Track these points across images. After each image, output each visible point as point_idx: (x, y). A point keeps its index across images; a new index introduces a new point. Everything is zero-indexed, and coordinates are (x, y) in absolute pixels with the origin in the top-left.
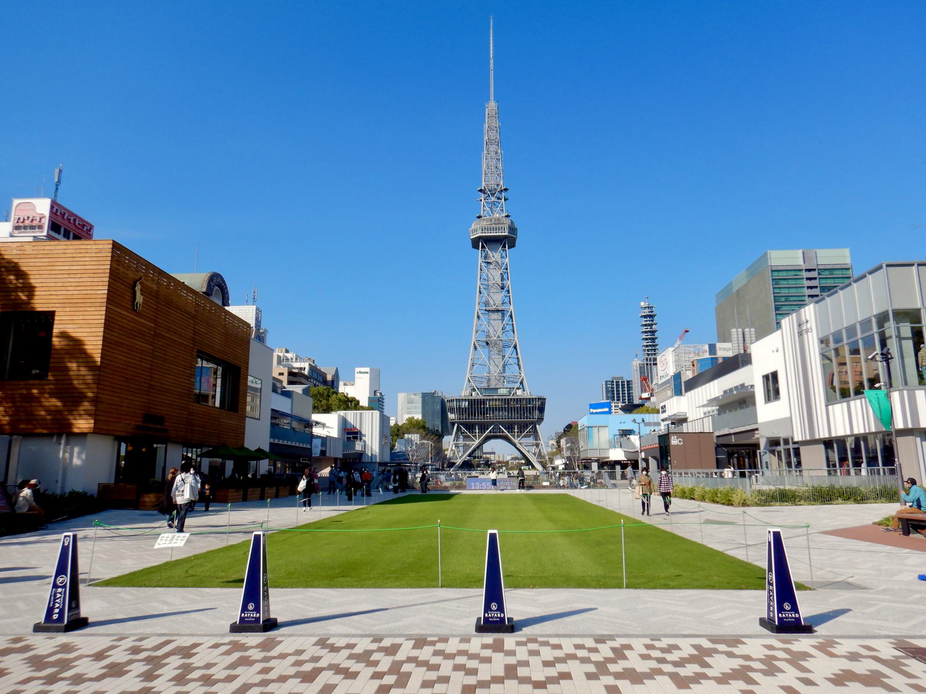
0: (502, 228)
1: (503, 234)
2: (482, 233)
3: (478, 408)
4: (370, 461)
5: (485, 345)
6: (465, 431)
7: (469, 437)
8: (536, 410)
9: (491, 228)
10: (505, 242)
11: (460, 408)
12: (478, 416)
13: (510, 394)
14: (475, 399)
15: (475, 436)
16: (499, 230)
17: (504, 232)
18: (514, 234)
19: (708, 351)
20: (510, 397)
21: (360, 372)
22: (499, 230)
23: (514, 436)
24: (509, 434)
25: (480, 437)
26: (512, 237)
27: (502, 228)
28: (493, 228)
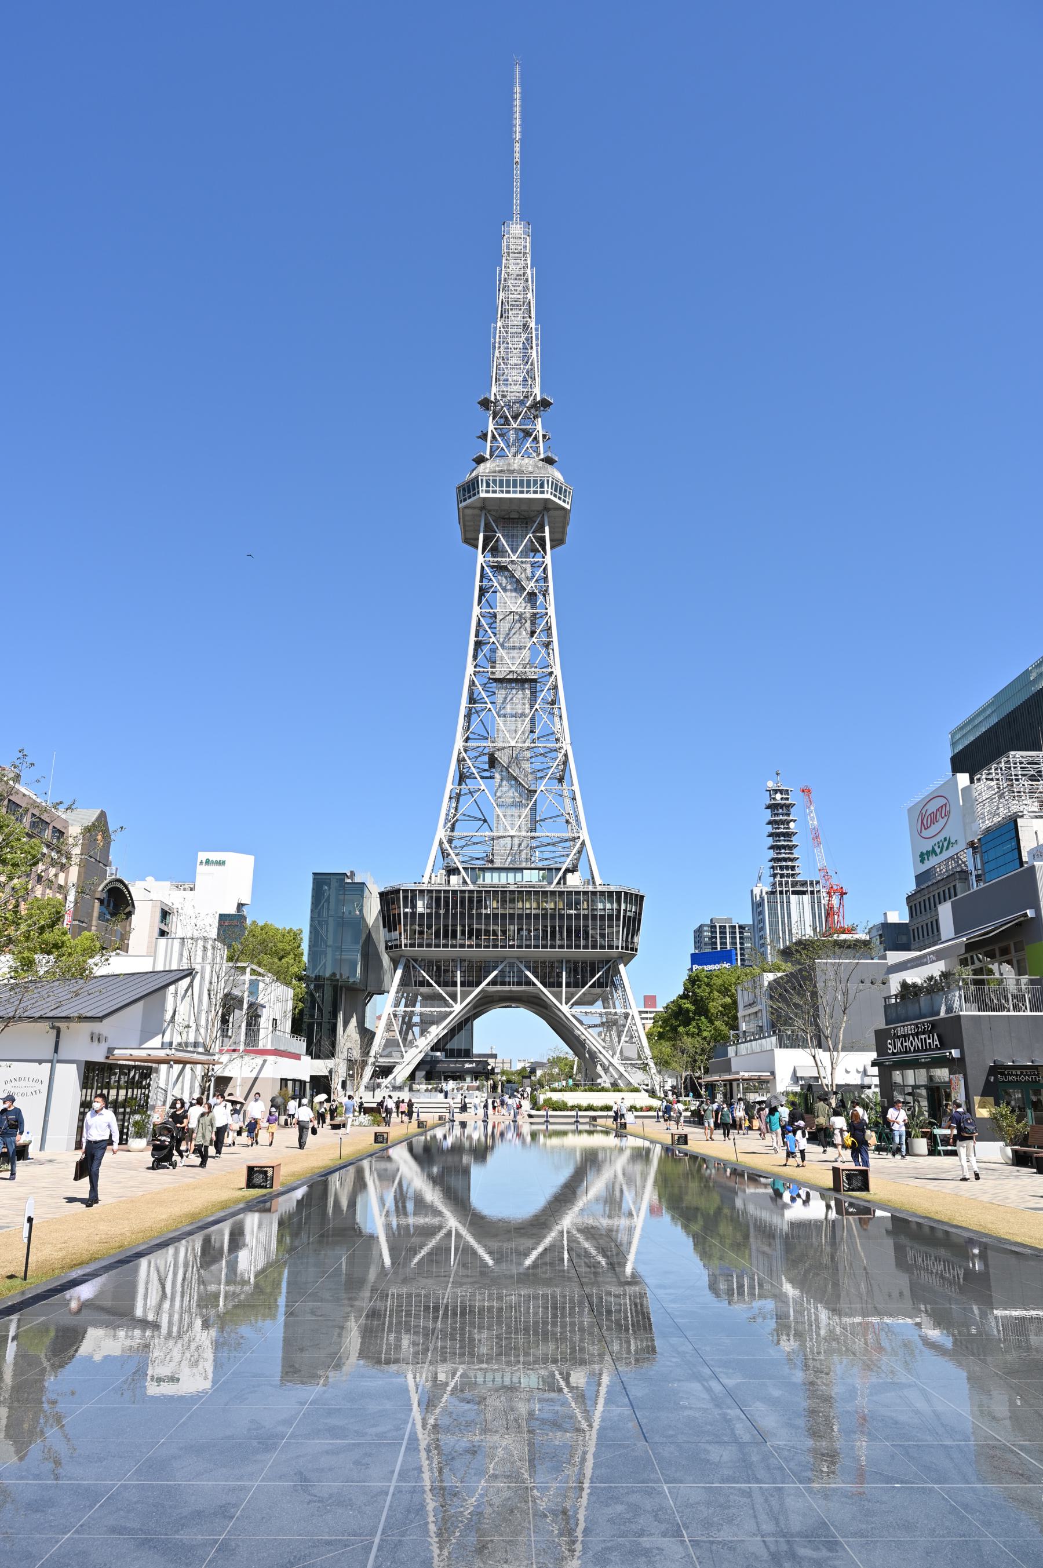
1: (539, 496)
2: (487, 492)
3: (462, 914)
5: (486, 767)
6: (428, 978)
7: (440, 997)
9: (508, 481)
13: (550, 883)
14: (455, 892)
15: (454, 997)
16: (529, 486)
17: (542, 492)
20: (552, 888)
21: (208, 862)
25: (464, 997)
27: (535, 482)
28: (515, 481)
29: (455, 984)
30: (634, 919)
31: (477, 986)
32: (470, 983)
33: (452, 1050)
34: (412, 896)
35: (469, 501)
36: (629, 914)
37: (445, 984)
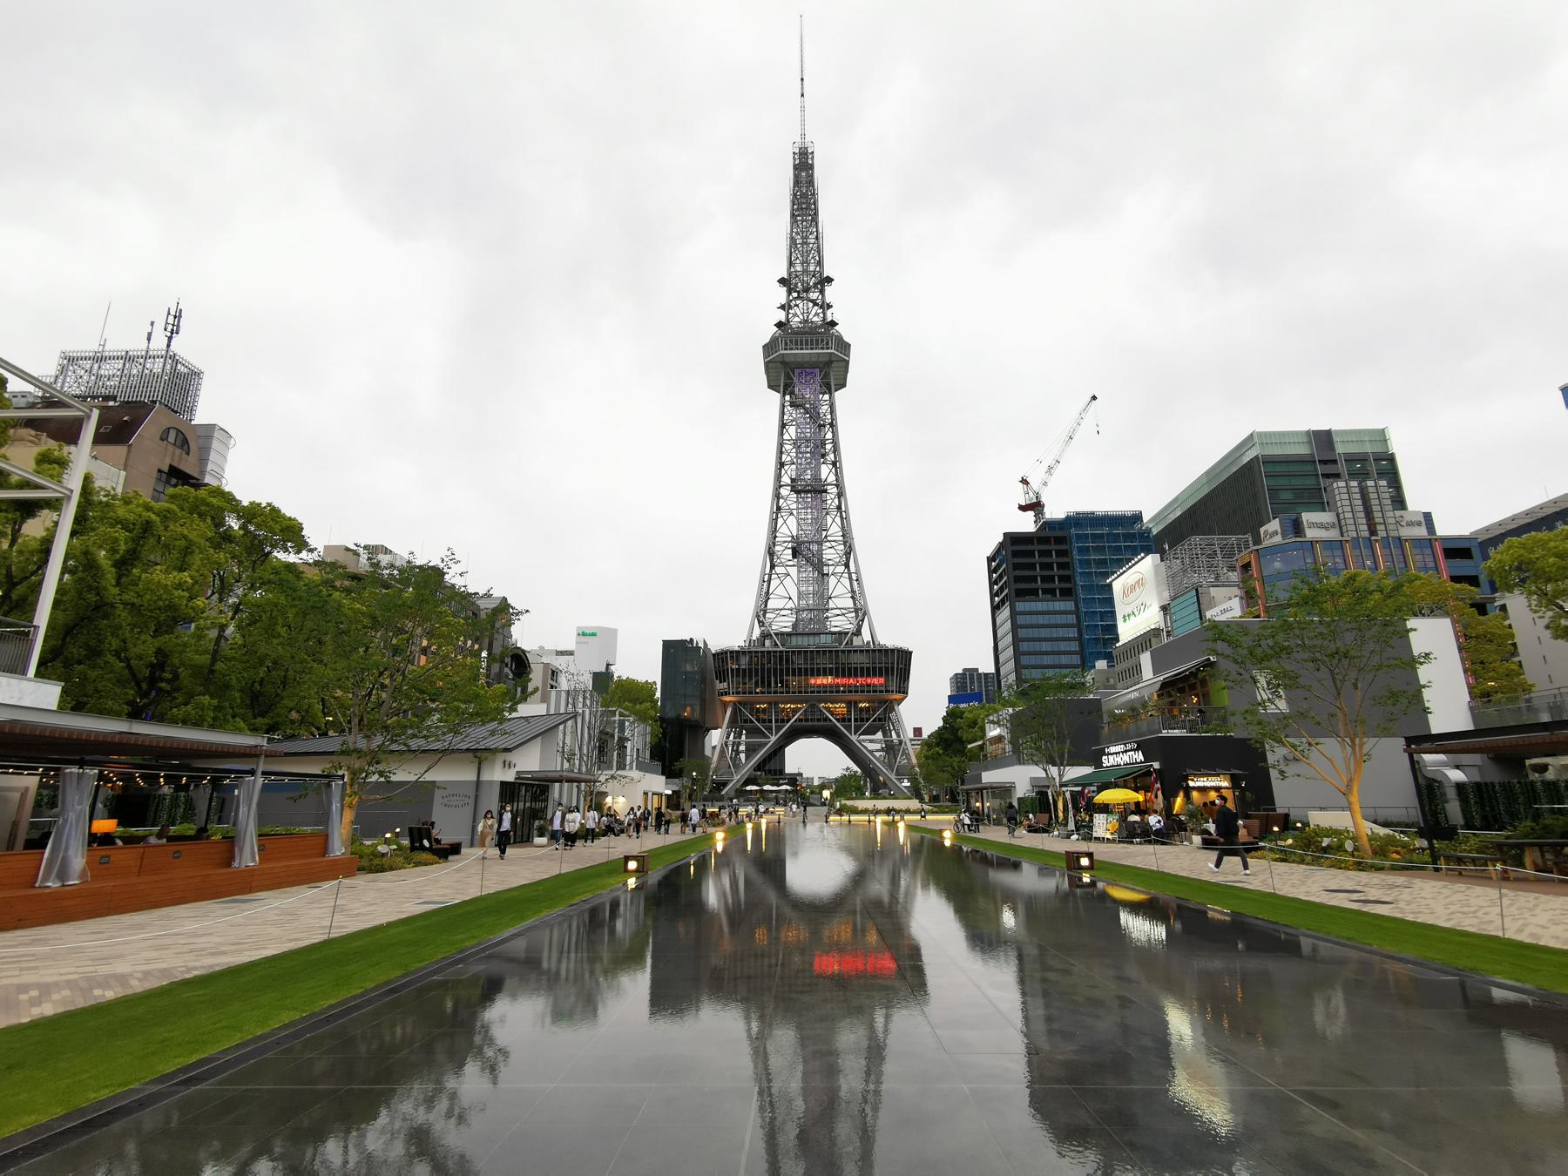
0: (822, 341)
2: (786, 349)
5: (790, 558)
8: (893, 674)
12: (776, 683)
14: (769, 652)
15: (769, 729)
16: (817, 344)
17: (828, 348)
18: (845, 355)
19: (1279, 531)
21: (584, 634)
22: (817, 344)
23: (848, 728)
24: (838, 724)
27: (822, 341)
28: (807, 341)
29: (770, 721)
30: (905, 669)
31: (788, 722)
33: (770, 771)
35: (771, 357)
36: (900, 666)
37: (764, 721)
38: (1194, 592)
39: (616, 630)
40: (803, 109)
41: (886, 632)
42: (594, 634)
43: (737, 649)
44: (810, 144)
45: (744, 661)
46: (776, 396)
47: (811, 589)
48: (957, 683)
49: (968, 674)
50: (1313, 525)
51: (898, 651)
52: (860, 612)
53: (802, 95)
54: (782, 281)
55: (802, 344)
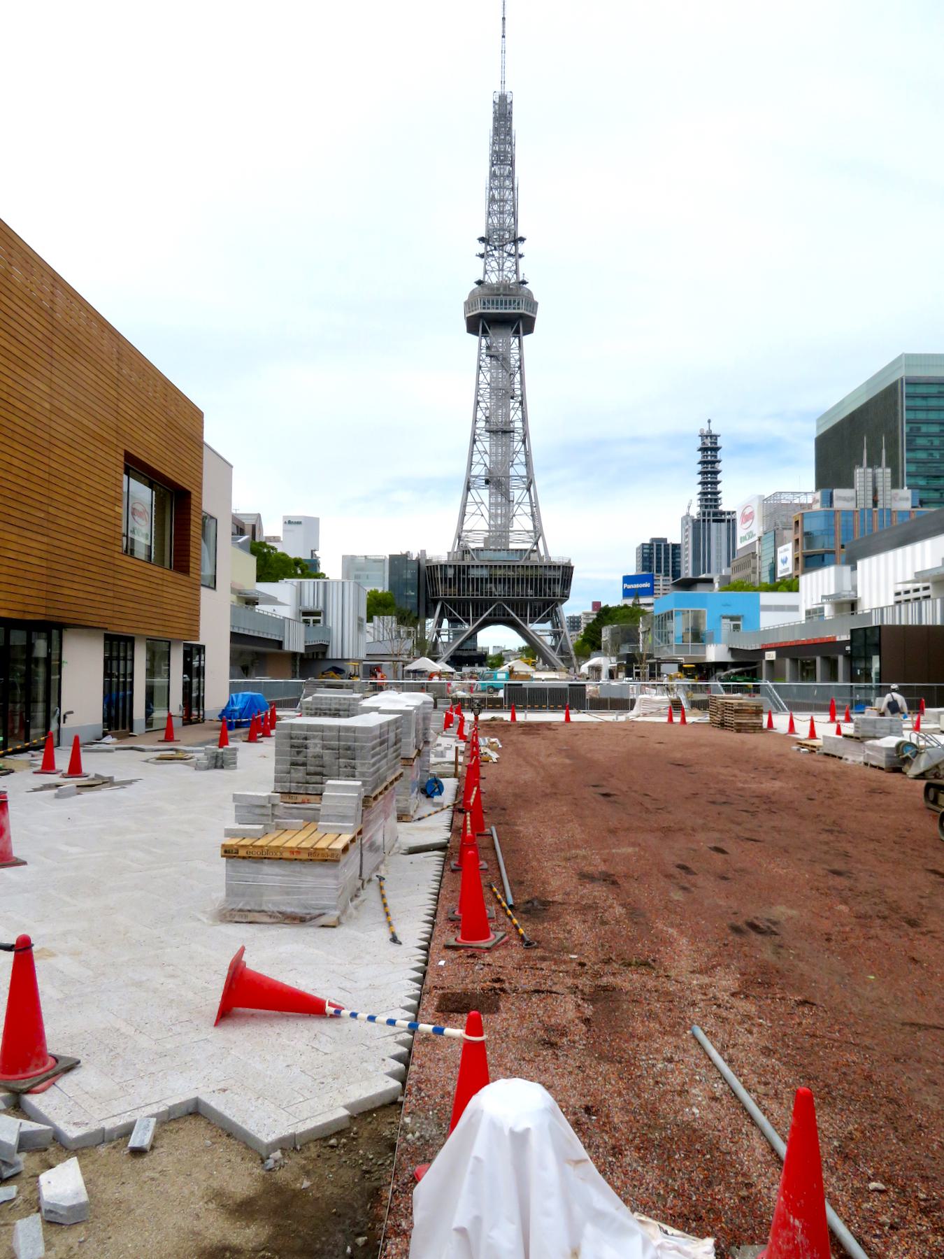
0: (515, 301)
2: (484, 308)
4: (340, 657)
10: (518, 326)
11: (446, 579)
12: (473, 591)
13: (521, 559)
16: (510, 304)
17: (519, 309)
18: (533, 312)
21: (290, 522)
25: (475, 621)
26: (531, 317)
27: (515, 301)
32: (477, 615)
34: (444, 567)
38: (773, 533)
39: (317, 520)
40: (503, 52)
41: (556, 550)
42: (299, 523)
43: (443, 563)
44: (509, 94)
45: (450, 573)
46: (474, 339)
47: (499, 511)
48: (643, 553)
49: (655, 544)
50: (840, 498)
51: (563, 567)
52: (537, 533)
53: (503, 37)
54: (482, 240)
55: (497, 304)
